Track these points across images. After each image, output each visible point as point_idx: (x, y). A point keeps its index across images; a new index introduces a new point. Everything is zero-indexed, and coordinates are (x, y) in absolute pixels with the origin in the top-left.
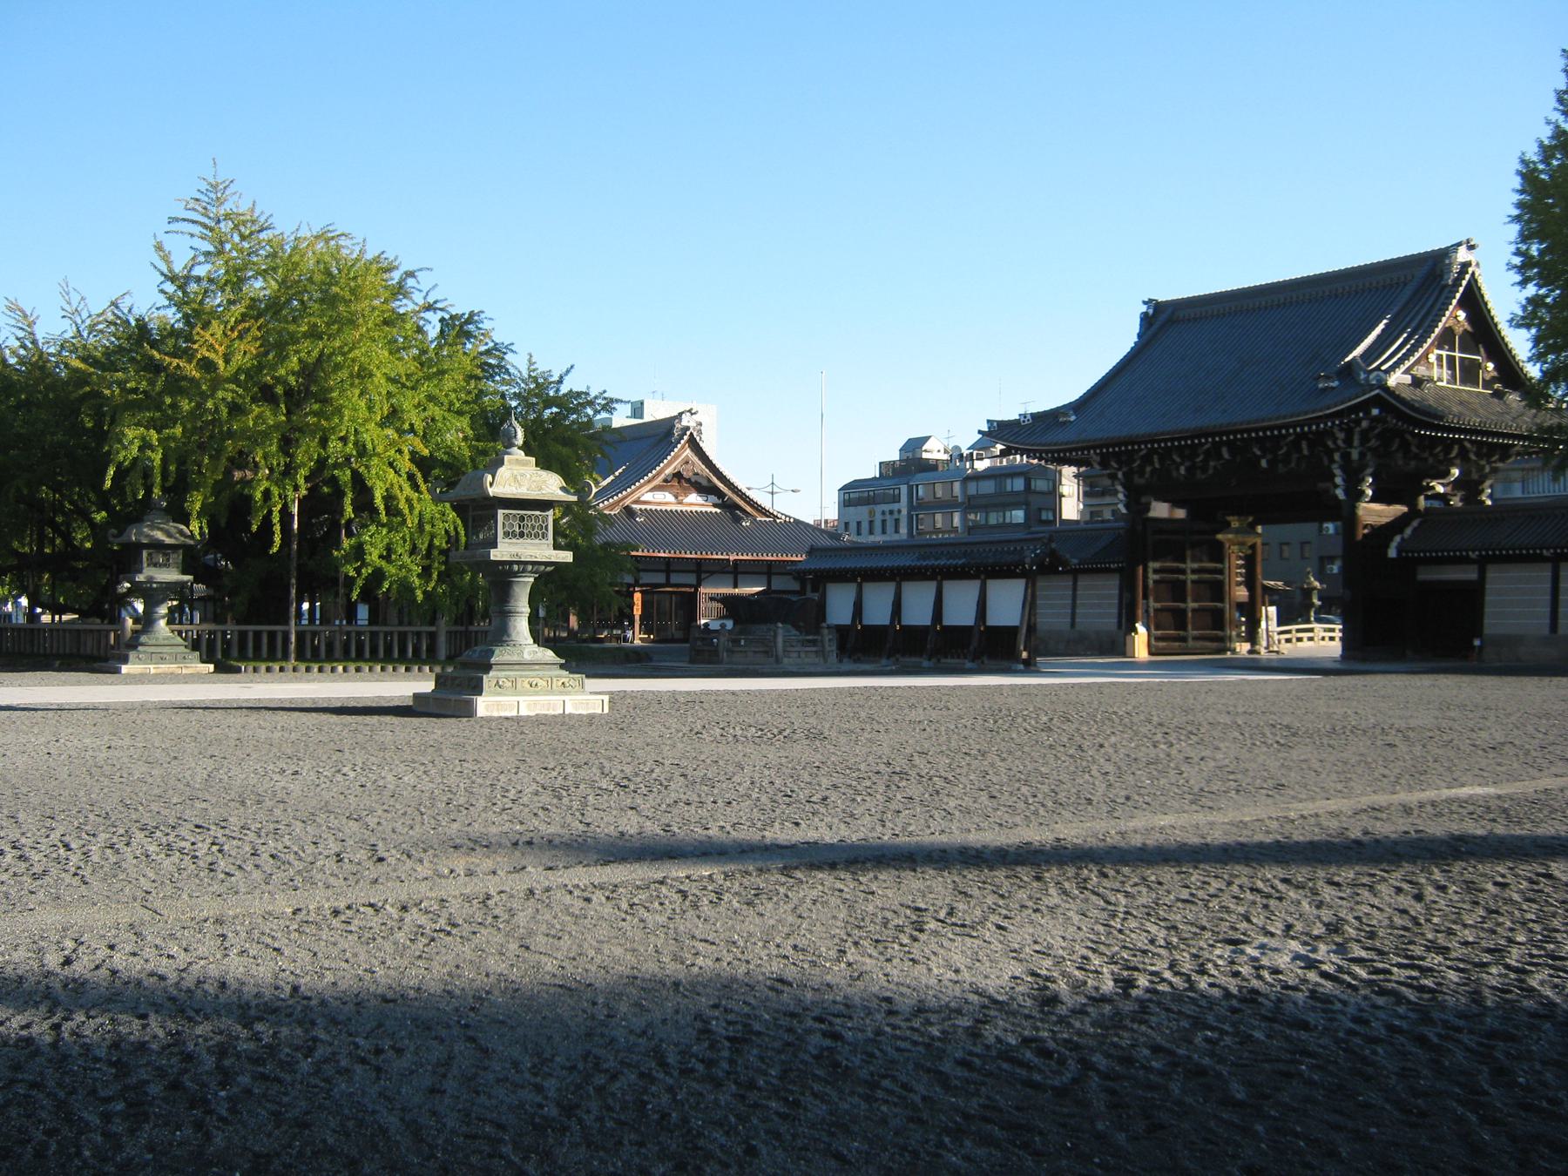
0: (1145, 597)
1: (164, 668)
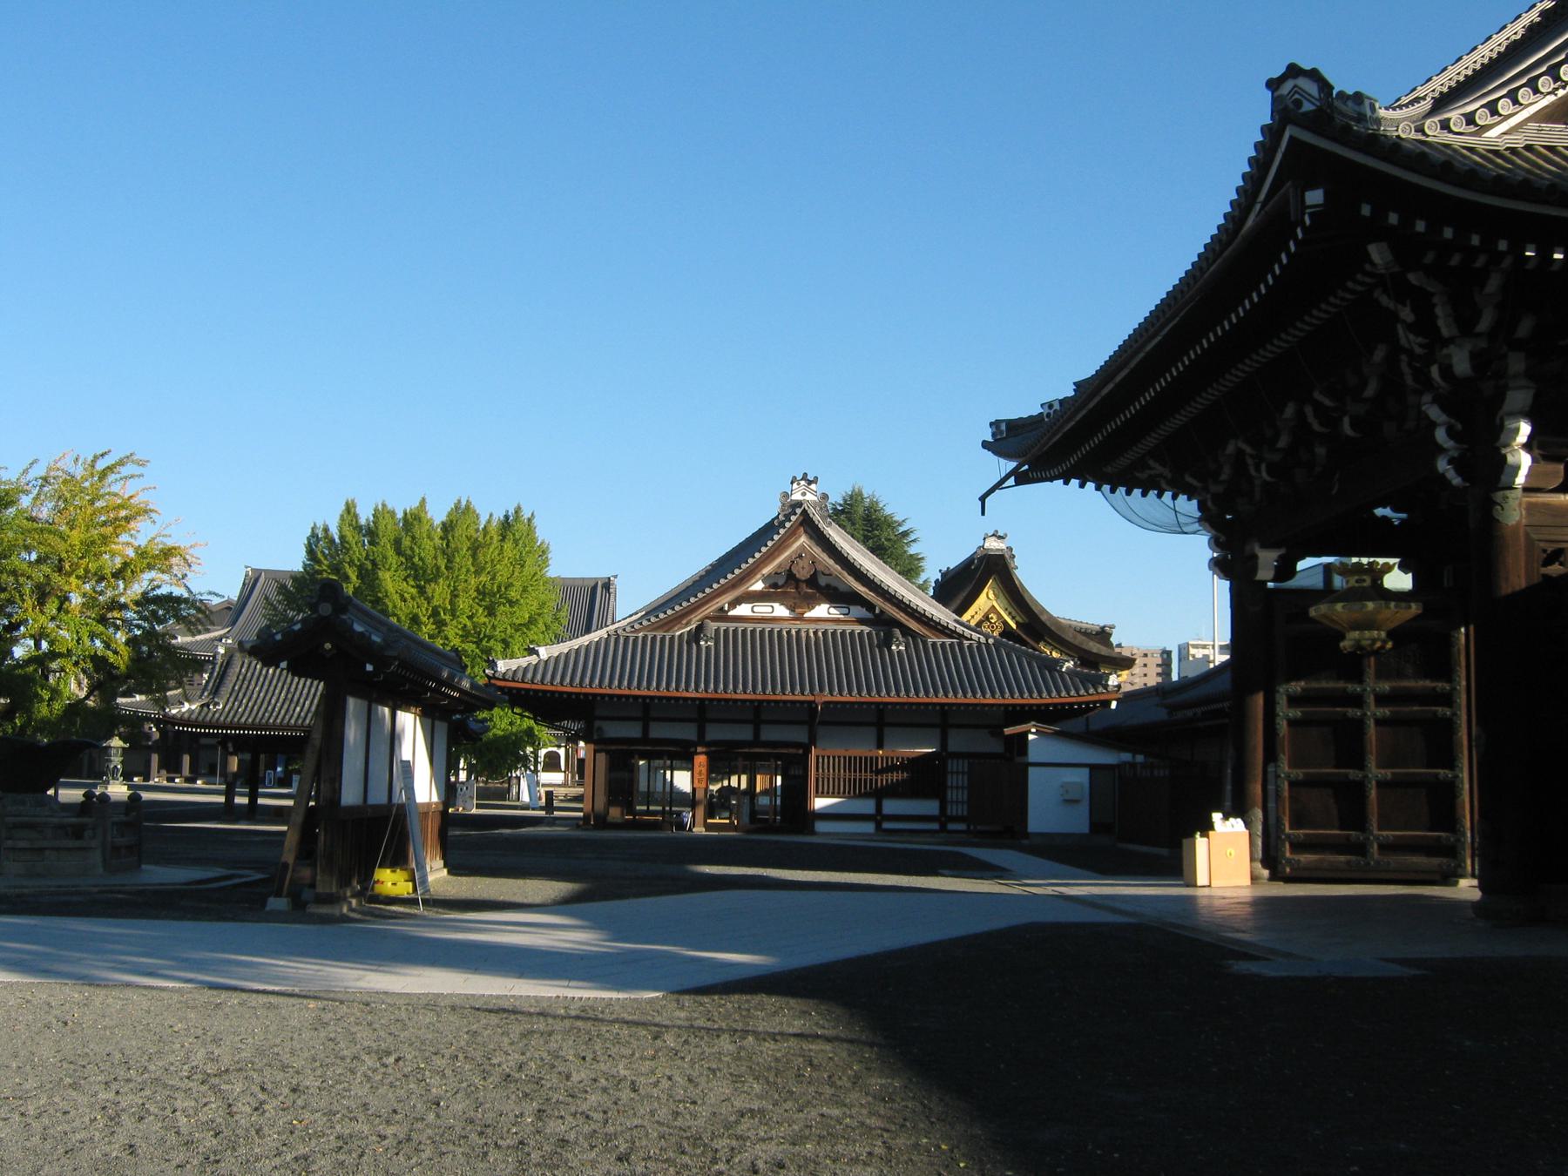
0: (1271, 755)
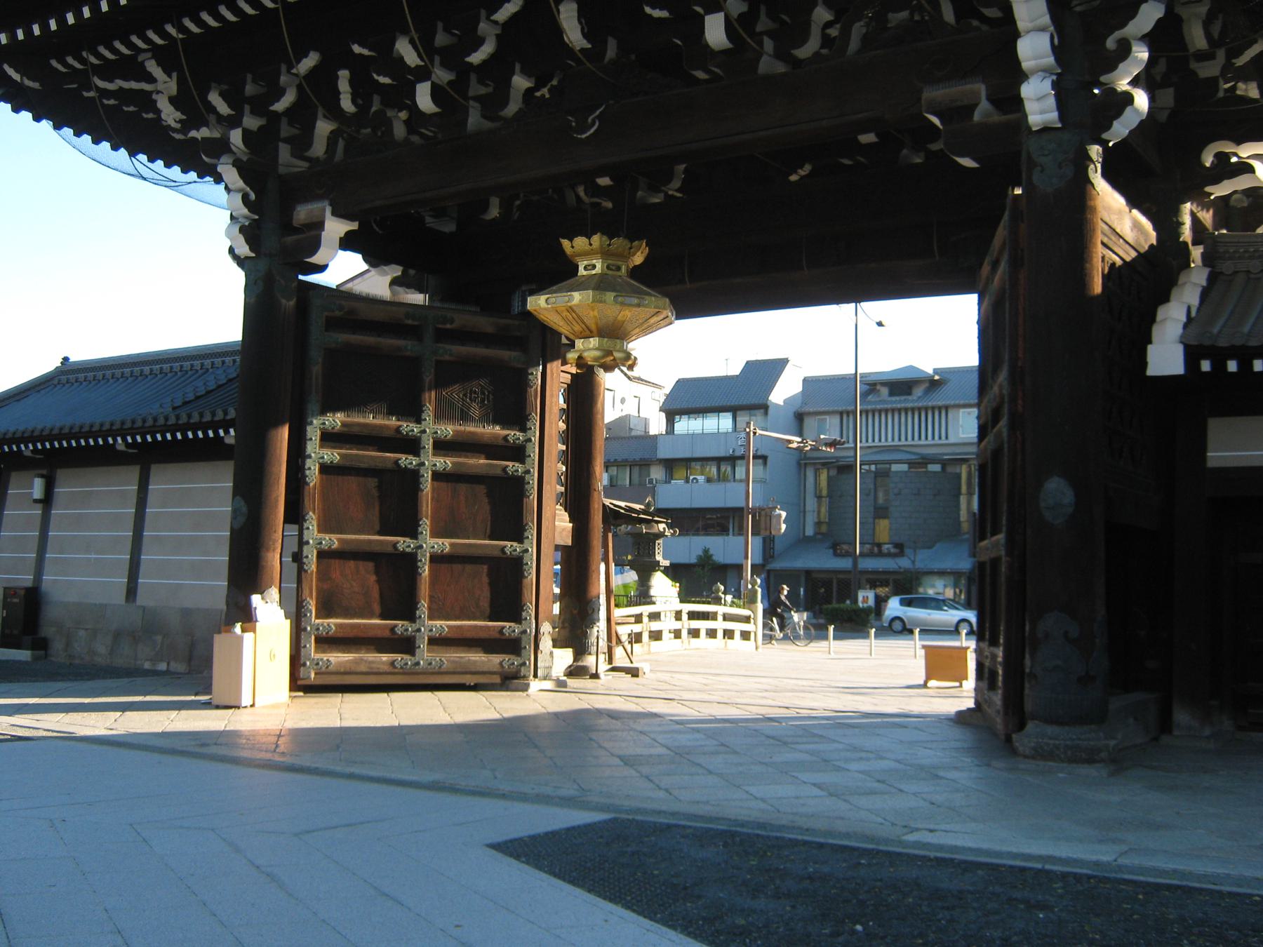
0: (294, 515)
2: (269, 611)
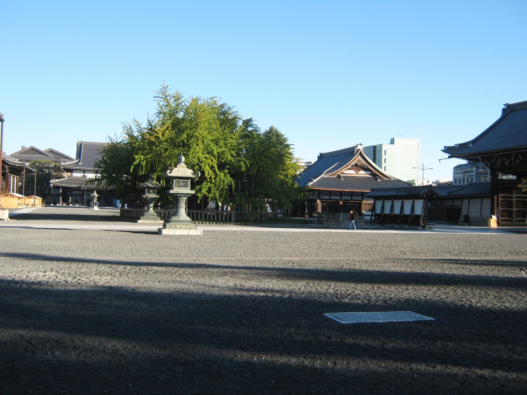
1: (150, 221)
2: (494, 218)
